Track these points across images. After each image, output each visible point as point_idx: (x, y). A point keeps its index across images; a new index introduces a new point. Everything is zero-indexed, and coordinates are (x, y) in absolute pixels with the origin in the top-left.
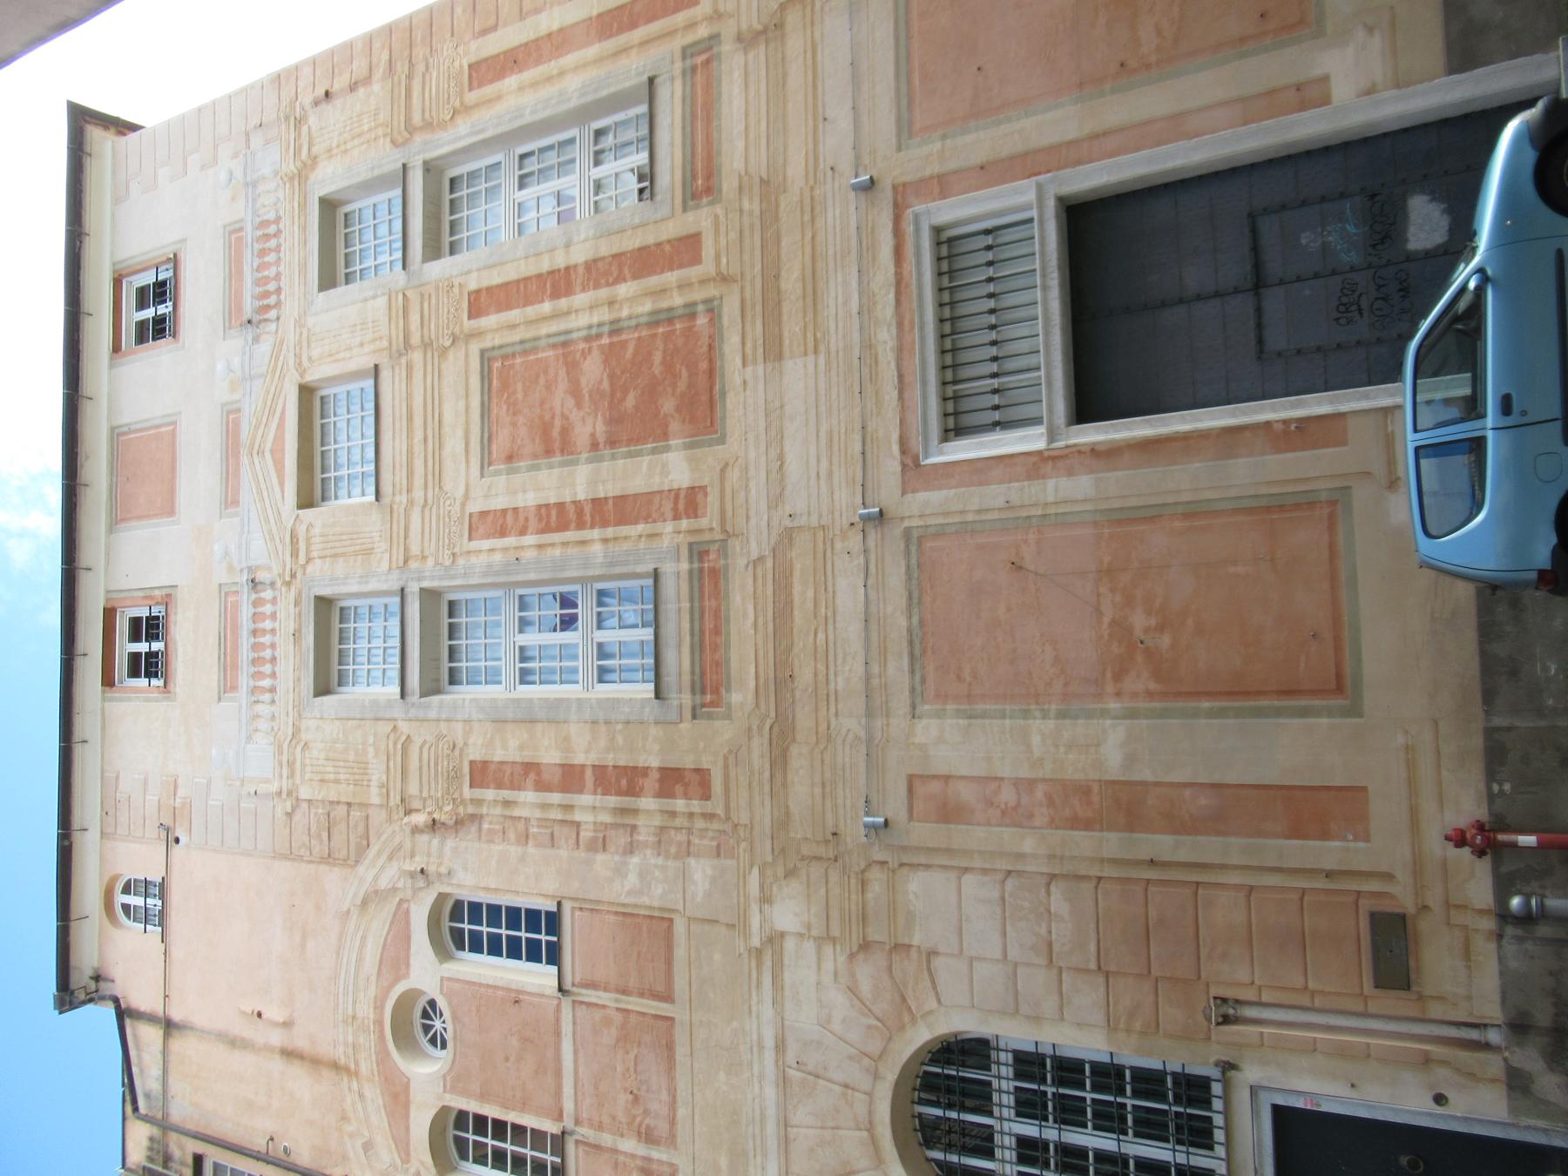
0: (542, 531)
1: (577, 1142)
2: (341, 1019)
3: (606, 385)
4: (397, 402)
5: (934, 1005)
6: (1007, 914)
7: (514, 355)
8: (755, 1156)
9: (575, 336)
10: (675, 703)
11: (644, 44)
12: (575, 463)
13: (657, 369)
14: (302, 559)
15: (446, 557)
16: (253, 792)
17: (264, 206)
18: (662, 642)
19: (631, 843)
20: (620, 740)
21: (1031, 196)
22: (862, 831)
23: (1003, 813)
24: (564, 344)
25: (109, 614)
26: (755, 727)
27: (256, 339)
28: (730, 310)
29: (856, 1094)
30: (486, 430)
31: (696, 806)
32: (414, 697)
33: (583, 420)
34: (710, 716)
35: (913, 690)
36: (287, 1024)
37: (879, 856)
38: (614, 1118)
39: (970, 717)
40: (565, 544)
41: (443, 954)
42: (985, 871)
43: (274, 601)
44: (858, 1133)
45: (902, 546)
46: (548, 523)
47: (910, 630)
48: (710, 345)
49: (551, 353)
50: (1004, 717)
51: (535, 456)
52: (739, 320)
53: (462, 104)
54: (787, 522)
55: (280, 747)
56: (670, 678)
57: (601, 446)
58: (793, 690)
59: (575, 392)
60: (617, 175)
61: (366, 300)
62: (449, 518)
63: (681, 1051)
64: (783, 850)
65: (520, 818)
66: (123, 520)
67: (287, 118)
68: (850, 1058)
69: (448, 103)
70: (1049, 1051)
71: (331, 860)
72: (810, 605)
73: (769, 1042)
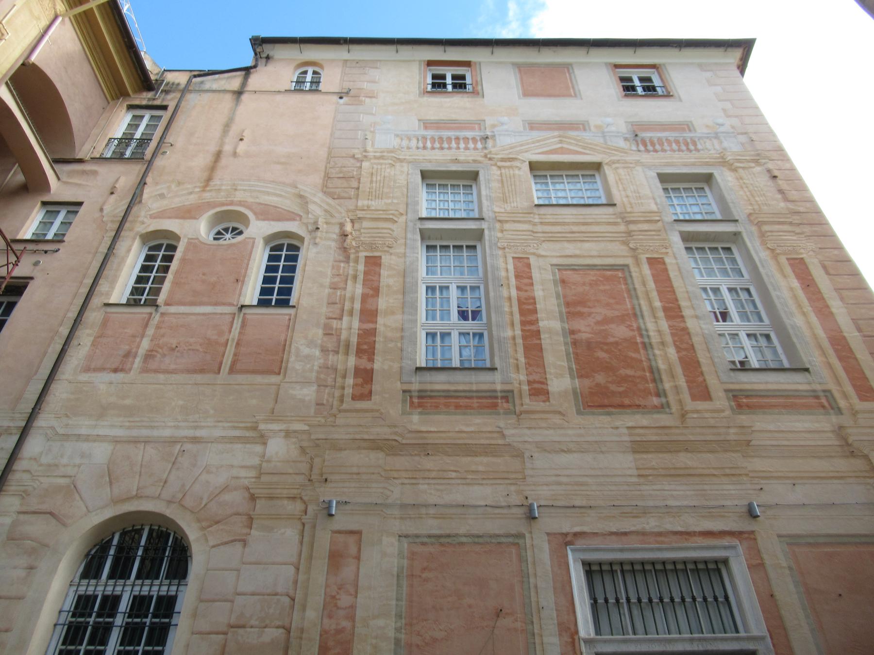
0: (519, 300)
1: (151, 314)
2: (236, 183)
3: (612, 340)
4: (594, 217)
5: (211, 543)
6: (266, 597)
7: (626, 284)
8: (129, 421)
9: (641, 321)
10: (413, 380)
11: (830, 366)
12: (562, 320)
13: (623, 372)
14: (499, 164)
15: (502, 244)
16: (367, 137)
17: (705, 143)
18: (451, 372)
19: (328, 351)
20: (391, 345)
21: (755, 632)
22: (327, 499)
23: (333, 597)
24: (635, 315)
25: (467, 64)
26: (397, 430)
27: (626, 139)
28: (664, 419)
29: (160, 488)
30: (580, 268)
31: (349, 391)
32: (419, 225)
33: (589, 326)
35: (417, 536)
36: (235, 154)
37: (310, 509)
38: (163, 336)
39: (398, 576)
40: (511, 314)
41: (268, 239)
42: (296, 582)
43: (475, 149)
44: (135, 488)
45: (512, 532)
46: (524, 303)
47: (456, 535)
48: (640, 406)
49: (629, 306)
50: (397, 600)
51: (565, 297)
52: (657, 425)
53: (778, 254)
54: (527, 455)
55: (391, 152)
56: (428, 377)
57: (573, 336)
58: (419, 455)
59: (606, 321)
60: (743, 348)
61: (654, 199)
63: (198, 378)
64: (317, 446)
65: (346, 285)
66: (520, 71)
67: (758, 155)
68: (183, 485)
69: (778, 246)
70: (173, 622)
71: (326, 178)
72: (473, 468)
73: (199, 433)
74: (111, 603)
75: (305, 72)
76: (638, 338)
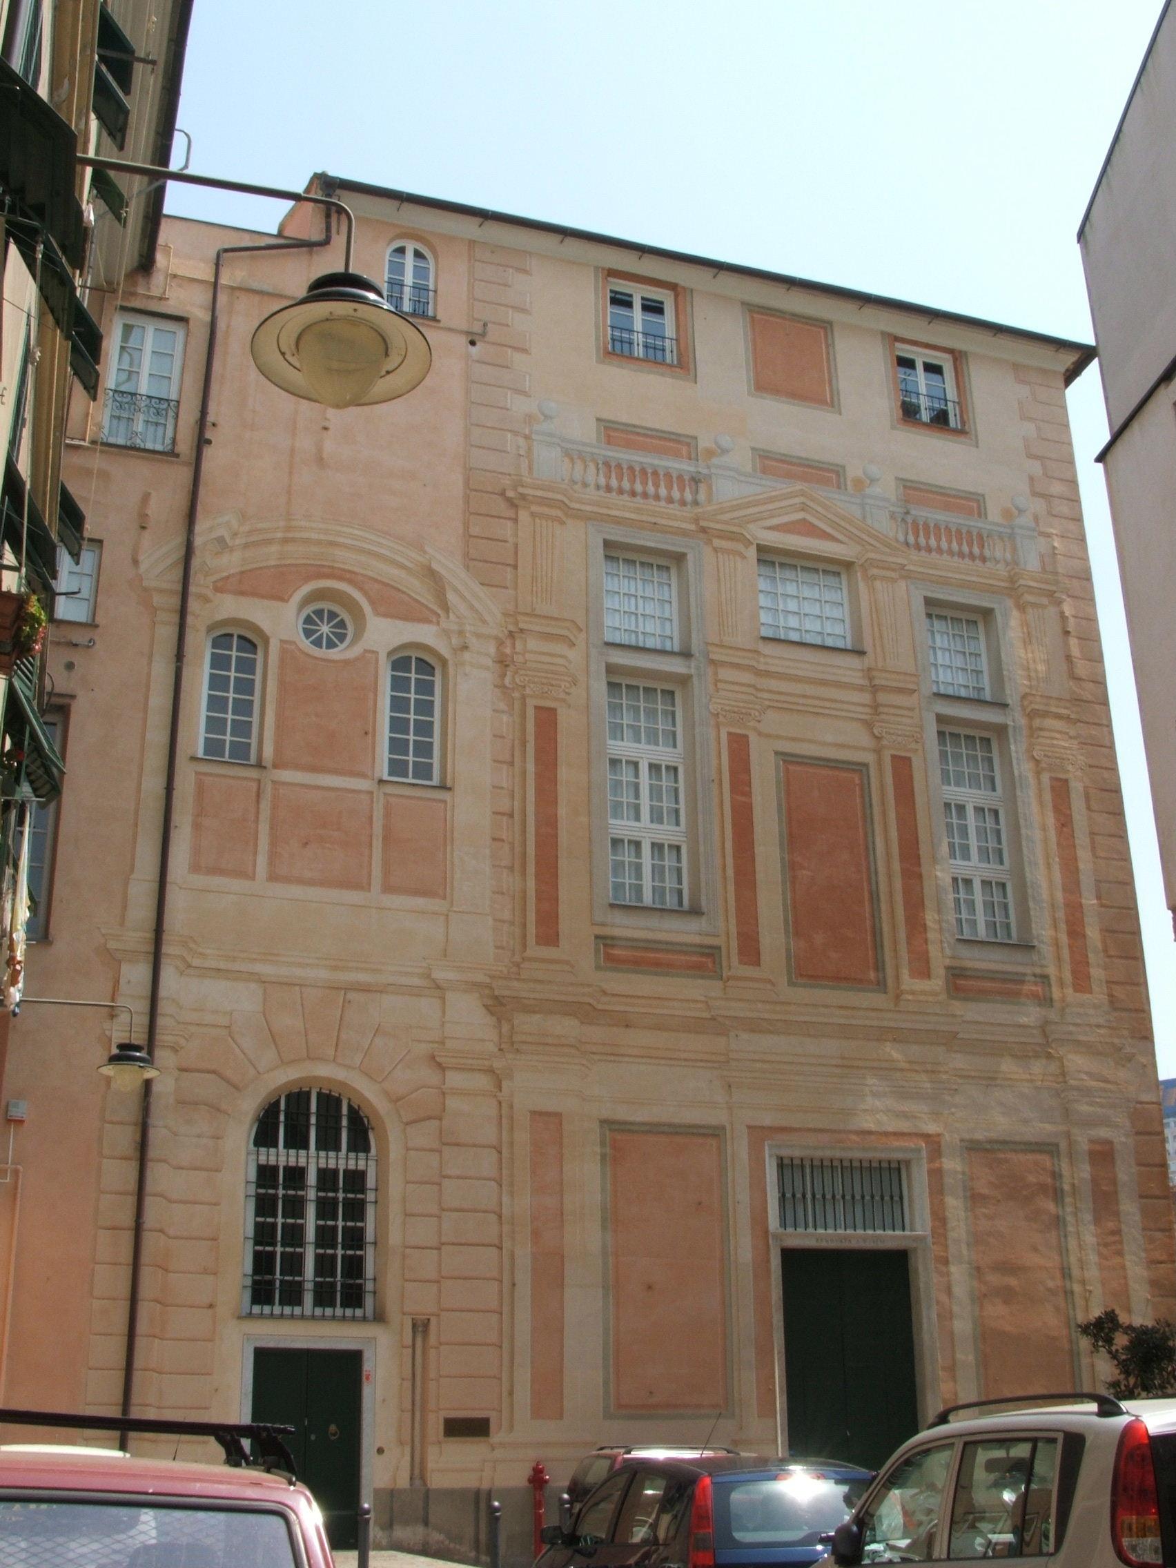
11: (1057, 944)
27: (893, 516)
34: (597, 951)
36: (320, 461)
62: (746, 714)
69: (1045, 756)
75: (401, 251)
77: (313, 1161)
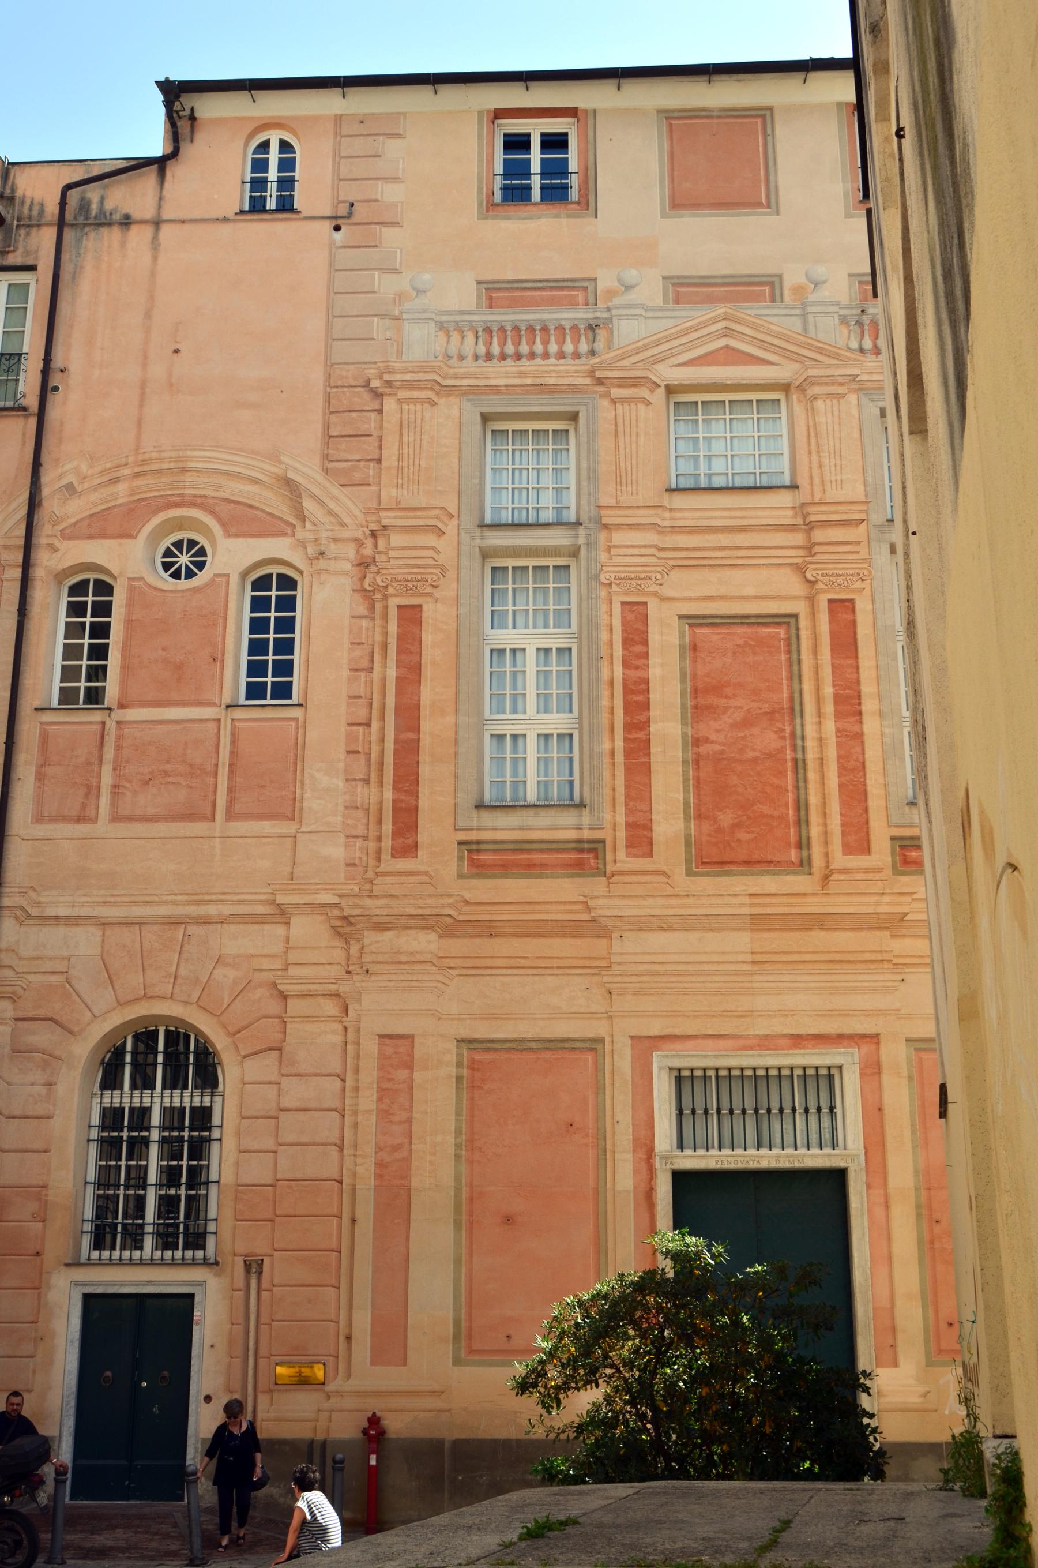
0: (625, 686)
1: (103, 723)
3: (750, 755)
15: (607, 575)
18: (524, 812)
27: (844, 321)
28: (797, 882)
29: (171, 986)
31: (387, 843)
34: (460, 858)
46: (633, 692)
48: (771, 862)
51: (694, 677)
62: (644, 579)
70: (216, 1134)
74: (141, 1115)
75: (265, 146)
76: (788, 752)
77: (157, 1100)
